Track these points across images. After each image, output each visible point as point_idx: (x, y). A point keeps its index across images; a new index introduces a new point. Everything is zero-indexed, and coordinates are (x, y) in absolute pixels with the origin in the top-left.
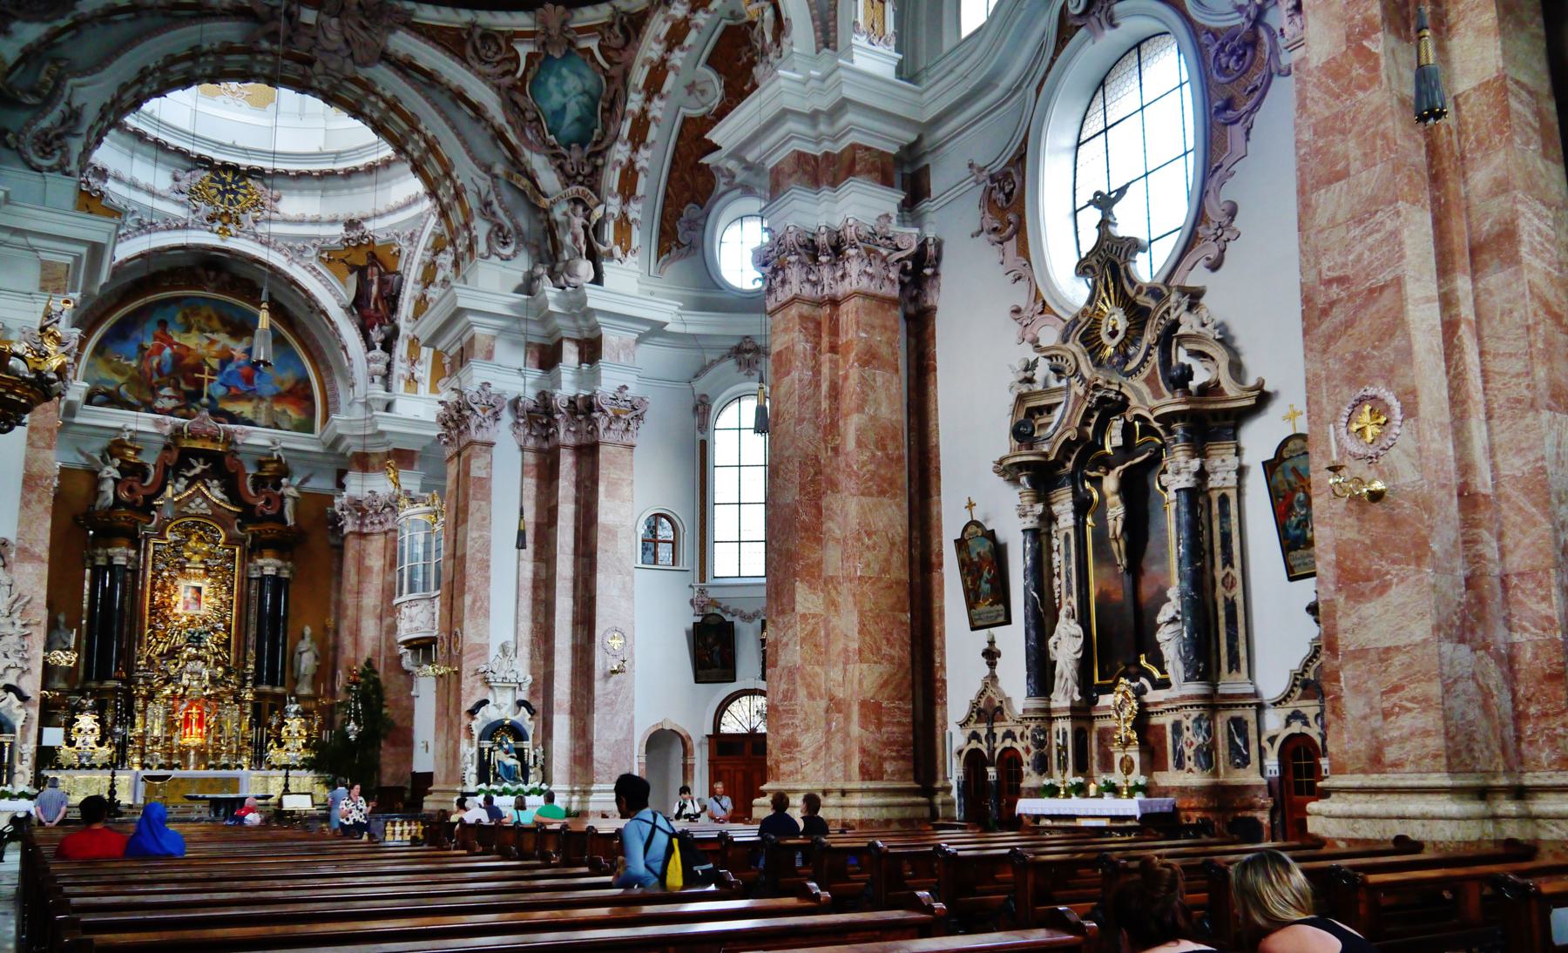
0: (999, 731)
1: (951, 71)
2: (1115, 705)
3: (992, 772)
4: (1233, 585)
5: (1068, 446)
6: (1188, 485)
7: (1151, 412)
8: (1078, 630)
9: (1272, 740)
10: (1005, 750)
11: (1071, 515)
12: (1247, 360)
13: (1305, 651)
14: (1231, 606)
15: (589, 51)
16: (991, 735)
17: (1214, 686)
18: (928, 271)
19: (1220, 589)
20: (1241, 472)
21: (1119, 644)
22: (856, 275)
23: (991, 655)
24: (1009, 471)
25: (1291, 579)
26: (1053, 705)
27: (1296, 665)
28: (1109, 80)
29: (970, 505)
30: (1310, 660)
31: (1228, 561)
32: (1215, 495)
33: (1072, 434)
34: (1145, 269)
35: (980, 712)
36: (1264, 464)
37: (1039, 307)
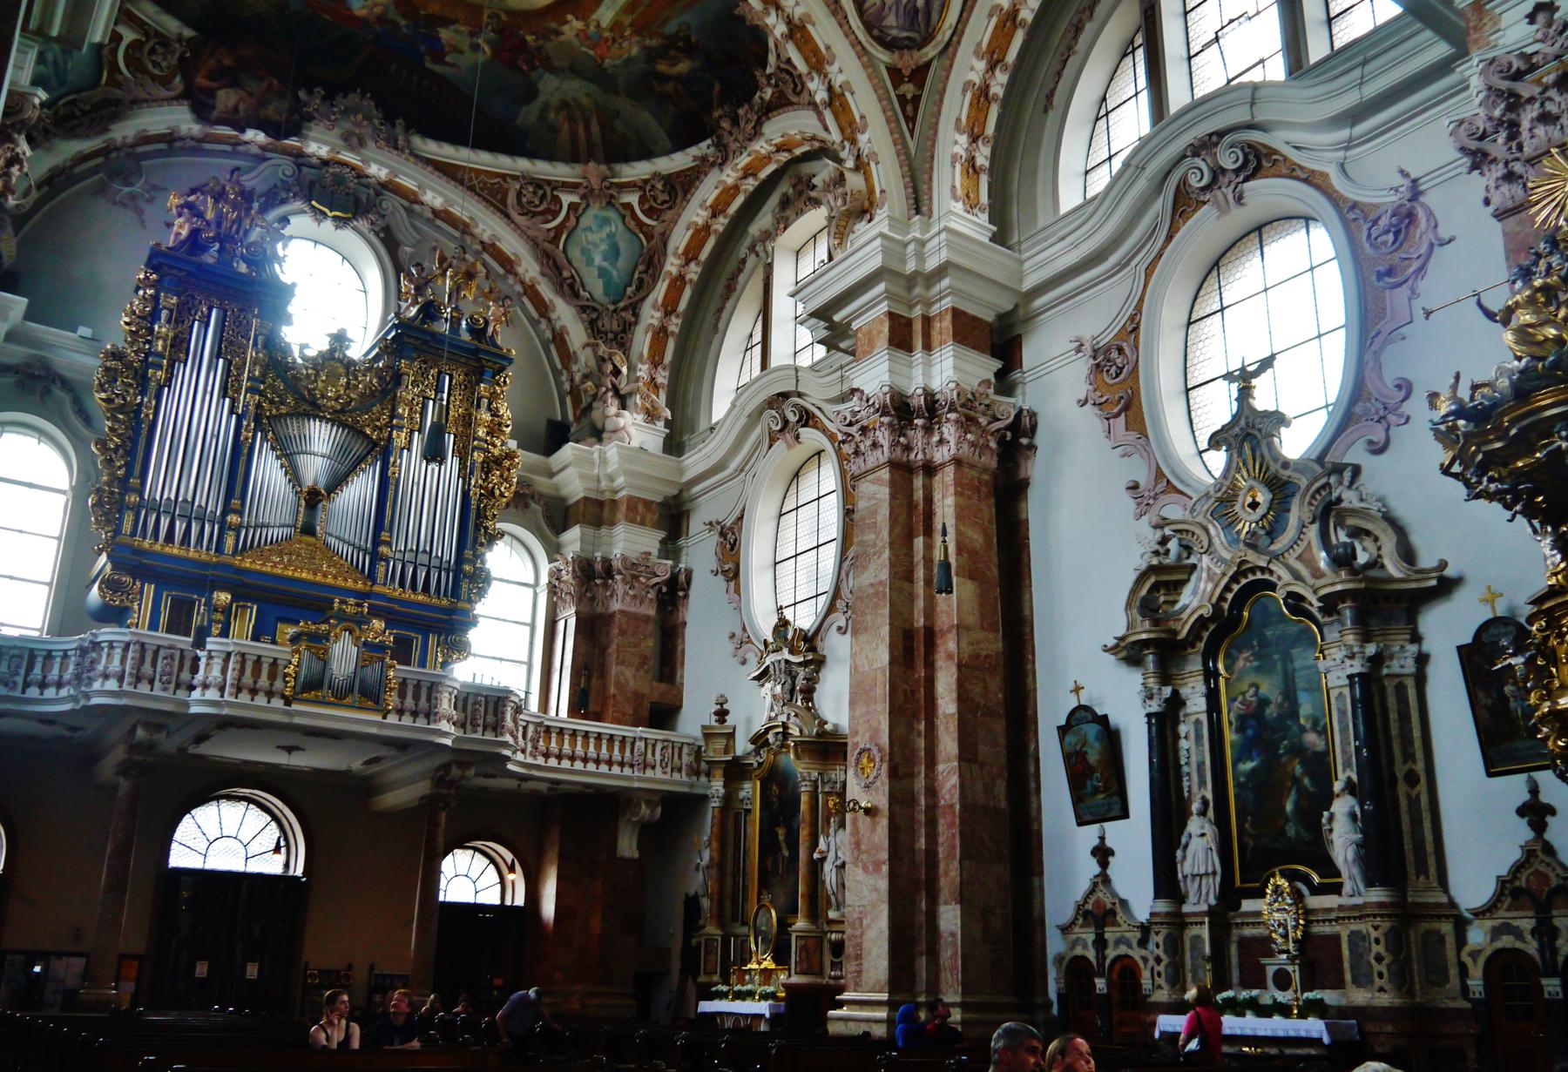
0: (1110, 934)
1: (1063, 238)
2: (1271, 911)
3: (1100, 983)
4: (1417, 781)
5: (1201, 623)
6: (1364, 670)
7: (1315, 592)
8: (1210, 830)
9: (1474, 954)
10: (1119, 958)
11: (1204, 700)
12: (1416, 539)
13: (1516, 855)
14: (1414, 802)
15: (629, 206)
16: (1101, 944)
17: (1404, 894)
18: (1024, 441)
19: (1402, 789)
20: (1422, 660)
21: (1270, 839)
22: (948, 443)
23: (1102, 853)
24: (1129, 653)
26: (1187, 908)
27: (1504, 871)
28: (1224, 261)
29: (1077, 690)
31: (1408, 756)
32: (1390, 686)
33: (1207, 611)
34: (1295, 443)
35: (1086, 915)
36: (1460, 648)
37: (1162, 485)
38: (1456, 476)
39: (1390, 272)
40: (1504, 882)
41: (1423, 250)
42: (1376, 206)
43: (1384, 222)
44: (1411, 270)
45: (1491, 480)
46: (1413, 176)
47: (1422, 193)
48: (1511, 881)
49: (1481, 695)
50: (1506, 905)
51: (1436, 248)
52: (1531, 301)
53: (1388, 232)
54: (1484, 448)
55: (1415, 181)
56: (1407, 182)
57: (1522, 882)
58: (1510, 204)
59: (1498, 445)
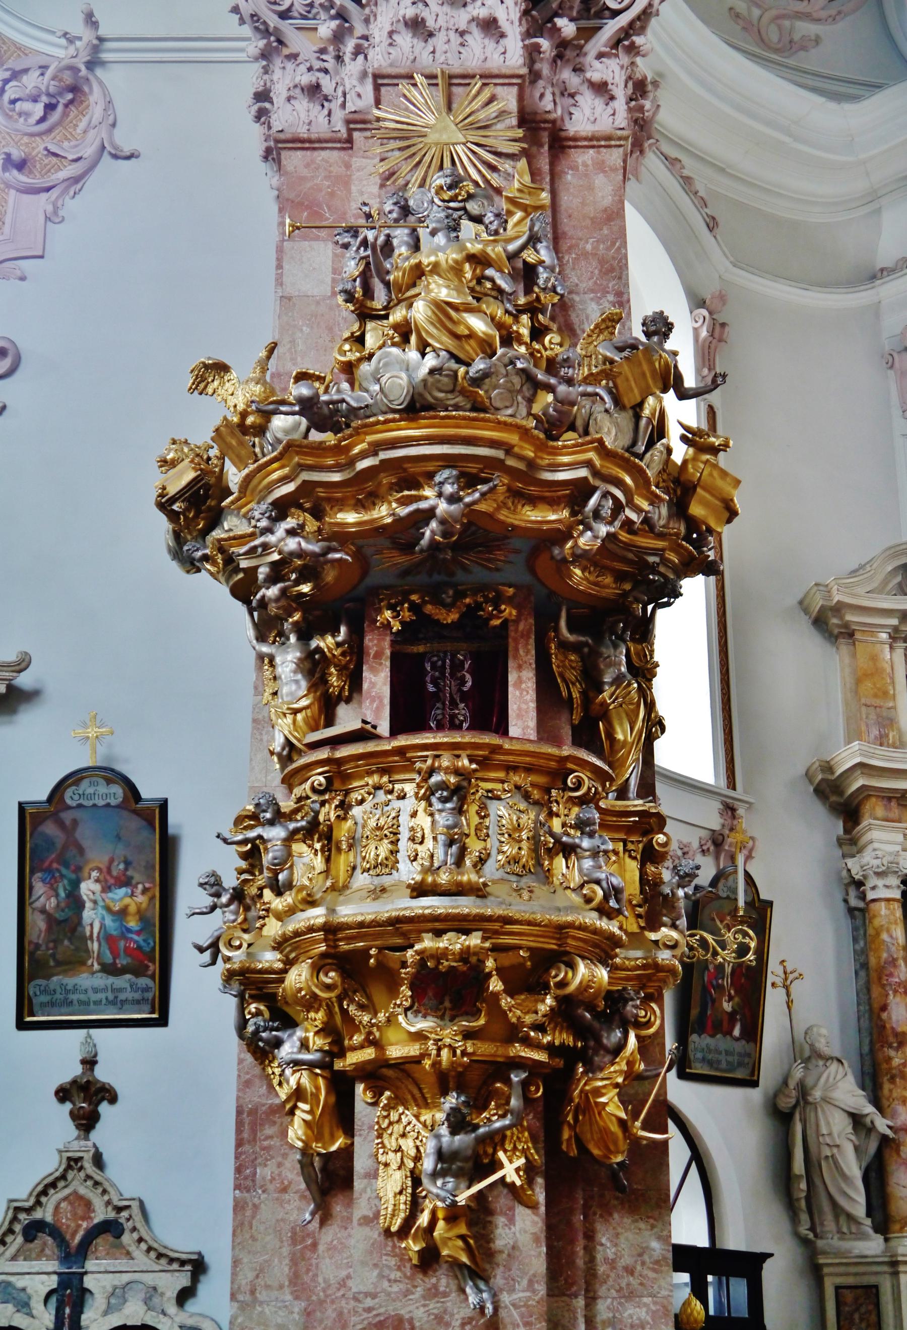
25: (21, 1025)
27: (23, 1190)
30: (53, 1185)
36: (22, 808)
38: (173, 516)
39: (21, 166)
40: (17, 1210)
41: (89, 151)
42: (21, 50)
43: (31, 81)
44: (62, 175)
45: (291, 533)
46: (102, 32)
47: (103, 63)
48: (28, 1210)
49: (39, 888)
50: (11, 1250)
51: (106, 157)
52: (457, 269)
53: (35, 100)
54: (305, 476)
55: (101, 40)
56: (88, 36)
57: (46, 1214)
58: (302, 131)
59: (336, 477)
